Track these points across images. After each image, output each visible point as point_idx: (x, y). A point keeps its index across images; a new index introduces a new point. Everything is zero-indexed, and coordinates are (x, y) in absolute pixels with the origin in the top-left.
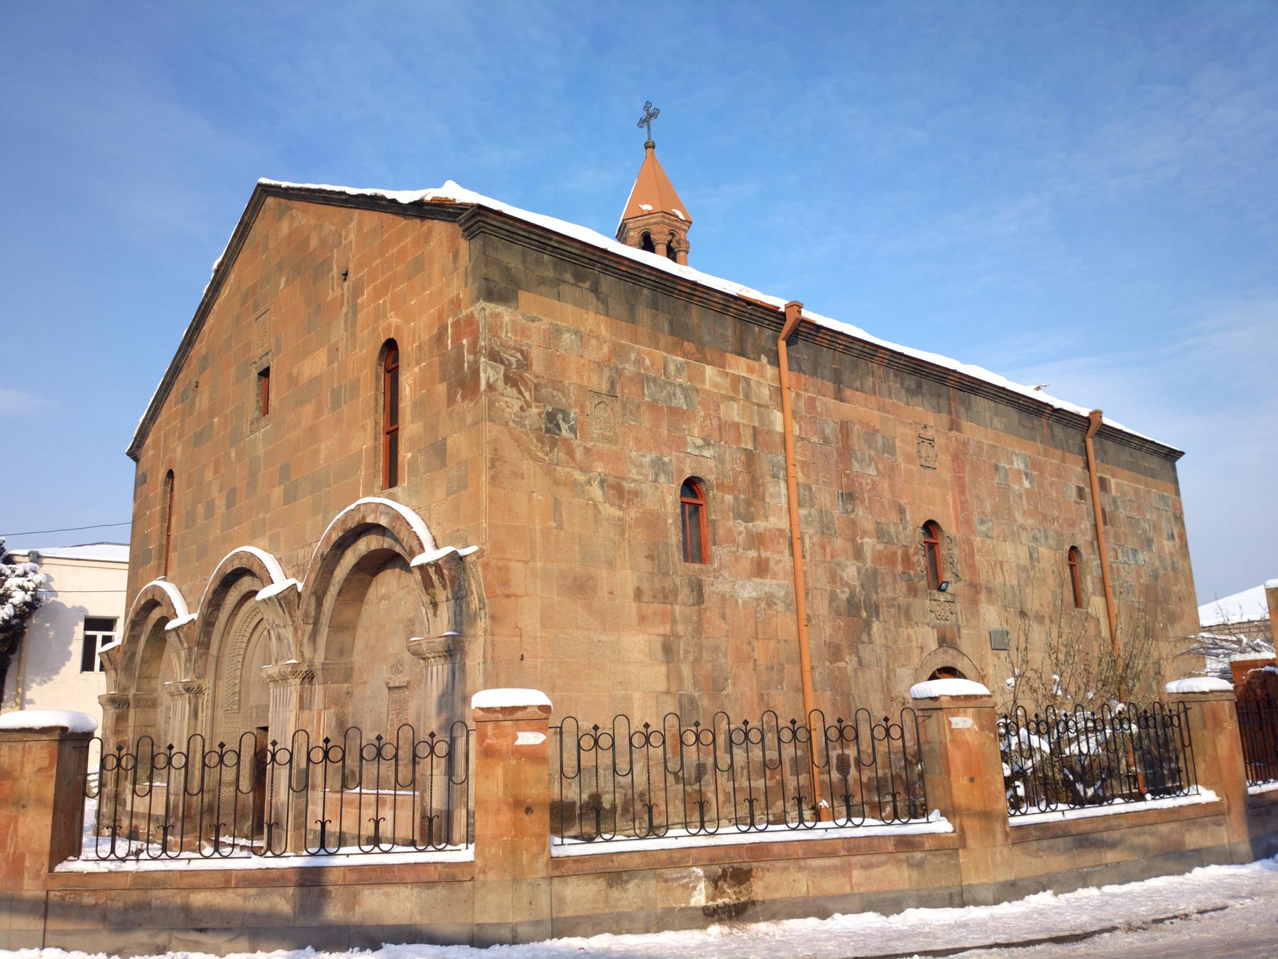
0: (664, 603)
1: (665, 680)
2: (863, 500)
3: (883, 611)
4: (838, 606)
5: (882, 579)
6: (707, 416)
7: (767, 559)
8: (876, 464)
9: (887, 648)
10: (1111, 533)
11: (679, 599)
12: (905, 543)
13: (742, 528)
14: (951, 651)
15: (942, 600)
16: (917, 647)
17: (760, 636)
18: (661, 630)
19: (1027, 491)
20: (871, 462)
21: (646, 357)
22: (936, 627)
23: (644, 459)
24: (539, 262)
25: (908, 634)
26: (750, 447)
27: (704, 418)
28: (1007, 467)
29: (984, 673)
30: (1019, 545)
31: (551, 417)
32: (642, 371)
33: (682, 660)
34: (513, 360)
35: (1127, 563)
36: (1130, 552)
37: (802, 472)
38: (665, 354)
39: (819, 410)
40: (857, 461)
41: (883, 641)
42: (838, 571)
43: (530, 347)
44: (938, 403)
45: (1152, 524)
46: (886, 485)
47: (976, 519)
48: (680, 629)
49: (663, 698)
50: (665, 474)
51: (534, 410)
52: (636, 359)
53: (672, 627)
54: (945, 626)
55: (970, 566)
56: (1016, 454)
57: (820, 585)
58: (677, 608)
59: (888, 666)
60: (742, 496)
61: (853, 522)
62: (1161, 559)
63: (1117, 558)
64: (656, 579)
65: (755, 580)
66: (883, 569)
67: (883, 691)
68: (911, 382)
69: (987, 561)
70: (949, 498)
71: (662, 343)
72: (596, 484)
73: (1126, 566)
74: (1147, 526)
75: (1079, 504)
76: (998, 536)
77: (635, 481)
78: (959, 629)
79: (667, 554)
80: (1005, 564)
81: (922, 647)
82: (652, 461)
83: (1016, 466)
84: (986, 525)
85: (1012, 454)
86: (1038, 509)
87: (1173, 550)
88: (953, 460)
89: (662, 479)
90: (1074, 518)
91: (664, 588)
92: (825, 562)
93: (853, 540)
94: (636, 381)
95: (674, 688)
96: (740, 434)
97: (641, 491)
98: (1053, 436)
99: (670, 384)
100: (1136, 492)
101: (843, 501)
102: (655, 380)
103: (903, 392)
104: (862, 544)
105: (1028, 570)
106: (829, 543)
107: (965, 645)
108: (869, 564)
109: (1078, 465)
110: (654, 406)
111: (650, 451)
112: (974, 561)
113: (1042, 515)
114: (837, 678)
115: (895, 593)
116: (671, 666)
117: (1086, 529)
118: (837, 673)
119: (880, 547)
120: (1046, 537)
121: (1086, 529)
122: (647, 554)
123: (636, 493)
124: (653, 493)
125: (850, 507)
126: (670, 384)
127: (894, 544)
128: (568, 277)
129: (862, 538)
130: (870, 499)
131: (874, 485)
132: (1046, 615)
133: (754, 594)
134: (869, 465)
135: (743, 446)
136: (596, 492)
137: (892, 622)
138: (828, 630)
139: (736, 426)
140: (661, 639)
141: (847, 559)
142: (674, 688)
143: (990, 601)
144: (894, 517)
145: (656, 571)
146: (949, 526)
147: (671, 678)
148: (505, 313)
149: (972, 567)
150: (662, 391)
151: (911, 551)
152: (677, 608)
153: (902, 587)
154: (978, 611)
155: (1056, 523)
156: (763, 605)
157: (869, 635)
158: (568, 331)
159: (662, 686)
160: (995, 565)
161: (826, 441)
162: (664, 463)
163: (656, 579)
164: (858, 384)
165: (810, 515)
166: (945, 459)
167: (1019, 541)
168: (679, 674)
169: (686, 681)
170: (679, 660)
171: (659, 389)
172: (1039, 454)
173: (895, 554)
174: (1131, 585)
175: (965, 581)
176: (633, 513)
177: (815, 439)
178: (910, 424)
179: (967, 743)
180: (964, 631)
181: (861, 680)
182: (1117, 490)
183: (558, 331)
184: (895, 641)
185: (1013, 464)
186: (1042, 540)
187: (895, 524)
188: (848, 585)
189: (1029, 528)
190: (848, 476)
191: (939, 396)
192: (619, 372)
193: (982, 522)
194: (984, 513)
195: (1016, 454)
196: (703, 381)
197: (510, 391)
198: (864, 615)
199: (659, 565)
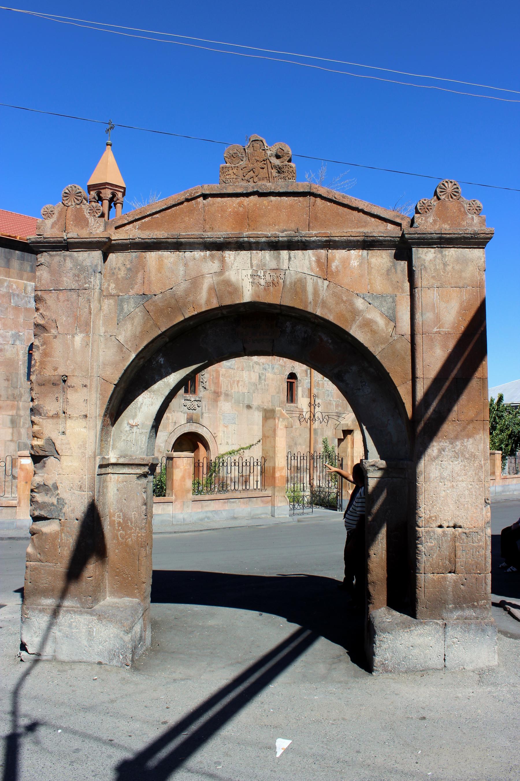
0: (13, 401)
1: (11, 435)
11: (23, 399)
14: (195, 424)
15: (192, 400)
16: (172, 422)
18: (10, 413)
21: (14, 284)
22: (187, 413)
23: (7, 334)
29: (216, 435)
30: (252, 372)
32: (11, 291)
33: (21, 426)
38: (26, 282)
48: (22, 413)
49: (8, 443)
50: (19, 340)
52: (7, 286)
53: (17, 412)
55: (216, 383)
58: (21, 404)
64: (9, 390)
71: (25, 276)
76: (238, 368)
78: (202, 414)
79: (17, 379)
80: (241, 382)
81: (175, 423)
82: (12, 334)
89: (18, 343)
91: (14, 394)
94: (7, 296)
95: (15, 439)
97: (5, 349)
99: (27, 297)
102: (18, 295)
107: (205, 421)
110: (17, 308)
111: (12, 330)
112: (219, 380)
116: (15, 430)
120: (273, 368)
122: (5, 378)
124: (12, 350)
126: (27, 297)
140: (10, 417)
142: (15, 439)
143: (226, 400)
145: (10, 386)
147: (14, 434)
149: (217, 384)
150: (22, 300)
152: (21, 404)
154: (217, 406)
155: (281, 361)
159: (9, 438)
160: (234, 382)
162: (19, 335)
163: (9, 390)
167: (252, 370)
168: (19, 434)
169: (23, 436)
170: (19, 427)
171: (20, 300)
175: (211, 390)
179: (27, 469)
180: (205, 415)
186: (270, 370)
189: (261, 364)
199: (11, 384)
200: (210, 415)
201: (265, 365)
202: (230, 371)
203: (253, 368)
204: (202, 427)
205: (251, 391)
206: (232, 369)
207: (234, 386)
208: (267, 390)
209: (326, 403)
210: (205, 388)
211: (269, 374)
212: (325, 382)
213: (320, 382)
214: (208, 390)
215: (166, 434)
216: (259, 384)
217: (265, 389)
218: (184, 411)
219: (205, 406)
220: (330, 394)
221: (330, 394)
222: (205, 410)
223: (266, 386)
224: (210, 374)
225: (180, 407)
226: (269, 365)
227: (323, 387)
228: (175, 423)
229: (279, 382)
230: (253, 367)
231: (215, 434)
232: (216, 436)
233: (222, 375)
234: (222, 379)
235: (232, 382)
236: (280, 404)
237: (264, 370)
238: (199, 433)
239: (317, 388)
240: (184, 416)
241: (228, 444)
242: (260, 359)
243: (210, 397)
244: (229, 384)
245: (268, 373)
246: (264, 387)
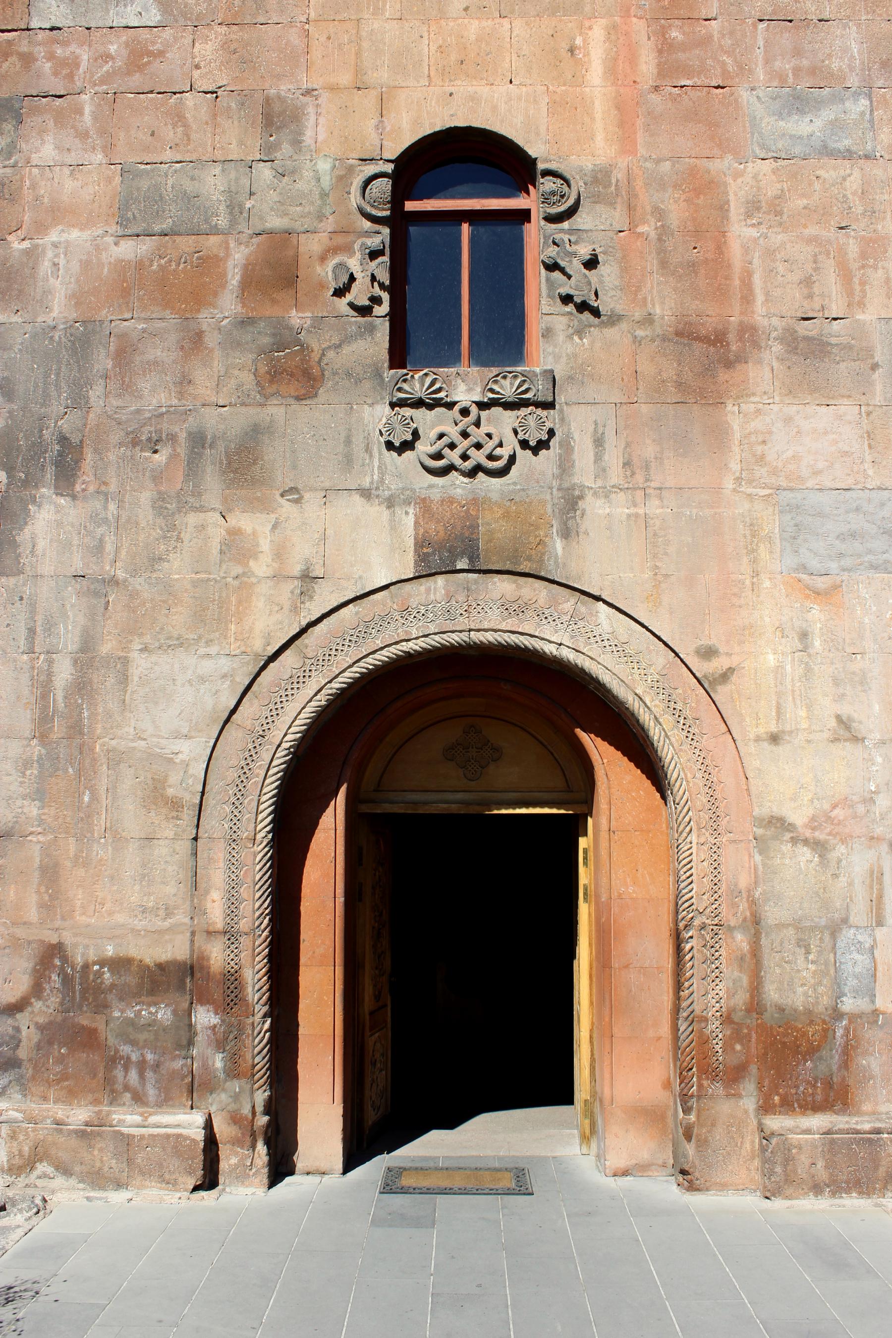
12: (275, 222)
14: (503, 586)
25: (235, 532)
54: (478, 502)
55: (693, 267)
59: (87, 645)
67: (42, 735)
69: (810, 240)
84: (828, 114)
104: (33, 255)
112: (720, 247)
115: (181, 395)
119: (128, 250)
127: (215, 231)
129: (41, 228)
137: (146, 497)
151: (312, 245)
175: (649, 320)
200: (654, 508)
202: (828, 174)
204: (569, 602)
206: (848, 155)
210: (583, 307)
214: (615, 319)
215: (225, 664)
218: (393, 485)
219: (599, 442)
222: (601, 472)
224: (630, 208)
225: (348, 461)
228: (308, 578)
231: (708, 653)
232: (725, 676)
233: (753, 207)
234: (753, 233)
235: (853, 249)
238: (549, 649)
240: (394, 526)
241: (857, 739)
243: (646, 367)
244: (829, 267)
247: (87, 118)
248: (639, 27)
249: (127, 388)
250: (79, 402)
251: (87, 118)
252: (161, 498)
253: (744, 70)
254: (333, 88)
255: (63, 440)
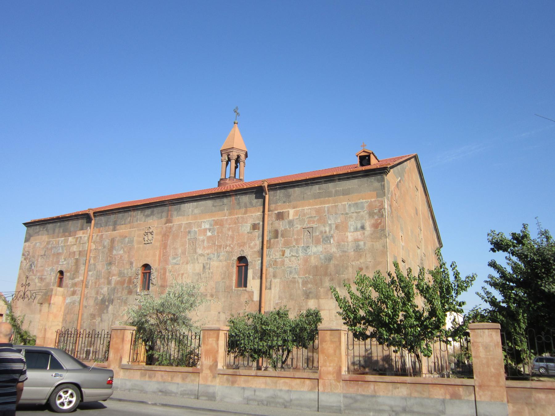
2: (115, 264)
3: (115, 302)
4: (97, 302)
5: (117, 290)
6: (67, 252)
7: (76, 290)
8: (124, 249)
9: (114, 314)
10: (282, 242)
12: (130, 275)
13: (70, 282)
17: (69, 313)
19: (209, 238)
20: (121, 249)
22: (139, 305)
24: (36, 229)
26: (78, 257)
27: (66, 253)
28: (196, 230)
31: (31, 265)
34: (26, 254)
35: (295, 256)
36: (300, 249)
37: (94, 260)
39: (104, 238)
40: (116, 250)
41: (112, 312)
42: (100, 290)
43: (30, 250)
44: (161, 216)
45: (334, 226)
46: (126, 256)
47: (170, 258)
51: (28, 264)
56: (204, 222)
57: (92, 296)
59: (112, 321)
60: (73, 273)
61: (109, 272)
62: (339, 245)
63: (283, 255)
65: (71, 297)
66: (118, 287)
68: (148, 212)
70: (157, 253)
72: (37, 278)
73: (293, 258)
74: (327, 229)
75: (251, 233)
76: (182, 263)
77: (45, 275)
83: (203, 227)
84: (177, 259)
85: (201, 223)
86: (215, 243)
87: (360, 237)
88: (163, 237)
89: (52, 273)
90: (246, 241)
92: (95, 288)
93: (108, 278)
96: (75, 254)
98: (239, 204)
100: (318, 211)
101: (107, 266)
102: (55, 247)
103: (144, 218)
104: (111, 279)
105: (200, 275)
106: (98, 281)
108: (113, 285)
109: (259, 211)
112: (165, 276)
113: (218, 246)
114: (92, 325)
117: (256, 245)
118: (92, 324)
119: (119, 279)
120: (218, 256)
121: (256, 245)
123: (45, 279)
125: (109, 268)
128: (42, 229)
129: (112, 277)
130: (118, 262)
131: (121, 257)
132: (208, 294)
133: (70, 301)
134: (120, 250)
135: (76, 258)
136: (37, 280)
138: (92, 310)
139: (74, 252)
141: (104, 285)
144: (128, 266)
146: (154, 266)
148: (27, 244)
151: (133, 278)
153: (126, 292)
155: (228, 248)
156: (72, 304)
157: (107, 310)
158: (38, 242)
160: (179, 275)
161: (104, 247)
162: (53, 269)
164: (123, 222)
165: (93, 273)
166: (159, 237)
172: (225, 216)
173: (125, 280)
174: (295, 269)
176: (44, 284)
177: (100, 248)
178: (143, 229)
181: (100, 326)
182: (294, 216)
183: (36, 243)
184: (118, 312)
185: (201, 227)
186: (215, 258)
187: (127, 269)
188: (103, 294)
189: (206, 255)
190: (111, 257)
191: (162, 212)
192: (47, 248)
193: (174, 258)
194: (177, 255)
195: (204, 222)
196: (67, 243)
197: (25, 261)
198: (107, 303)
201: (210, 255)
203: (197, 260)
205: (195, 281)
206: (178, 264)
207: (178, 278)
208: (212, 277)
209: (287, 282)
211: (214, 263)
212: (285, 259)
213: (277, 260)
214: (156, 285)
216: (203, 273)
217: (209, 277)
220: (294, 271)
221: (294, 271)
223: (211, 274)
224: (158, 272)
226: (214, 254)
227: (283, 265)
229: (224, 269)
230: (197, 259)
235: (177, 275)
236: (225, 290)
237: (209, 260)
239: (274, 267)
242: (205, 251)
245: (213, 261)
246: (208, 276)
247: (116, 264)
248: (162, 250)
249: (117, 294)
250: (114, 295)
251: (116, 264)
252: (119, 305)
253: (170, 255)
254: (136, 260)
255: (112, 299)
